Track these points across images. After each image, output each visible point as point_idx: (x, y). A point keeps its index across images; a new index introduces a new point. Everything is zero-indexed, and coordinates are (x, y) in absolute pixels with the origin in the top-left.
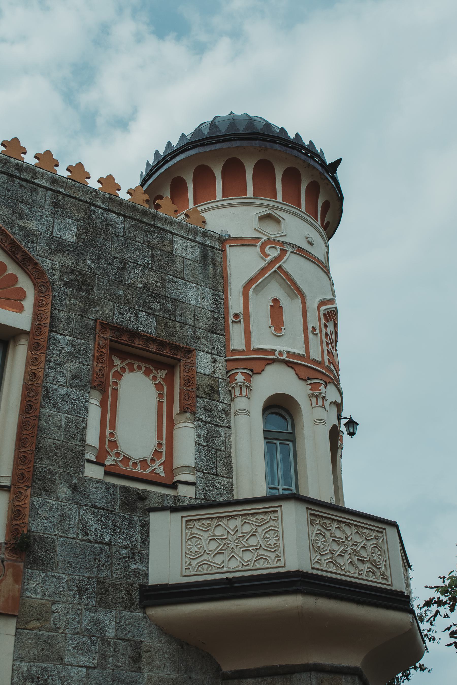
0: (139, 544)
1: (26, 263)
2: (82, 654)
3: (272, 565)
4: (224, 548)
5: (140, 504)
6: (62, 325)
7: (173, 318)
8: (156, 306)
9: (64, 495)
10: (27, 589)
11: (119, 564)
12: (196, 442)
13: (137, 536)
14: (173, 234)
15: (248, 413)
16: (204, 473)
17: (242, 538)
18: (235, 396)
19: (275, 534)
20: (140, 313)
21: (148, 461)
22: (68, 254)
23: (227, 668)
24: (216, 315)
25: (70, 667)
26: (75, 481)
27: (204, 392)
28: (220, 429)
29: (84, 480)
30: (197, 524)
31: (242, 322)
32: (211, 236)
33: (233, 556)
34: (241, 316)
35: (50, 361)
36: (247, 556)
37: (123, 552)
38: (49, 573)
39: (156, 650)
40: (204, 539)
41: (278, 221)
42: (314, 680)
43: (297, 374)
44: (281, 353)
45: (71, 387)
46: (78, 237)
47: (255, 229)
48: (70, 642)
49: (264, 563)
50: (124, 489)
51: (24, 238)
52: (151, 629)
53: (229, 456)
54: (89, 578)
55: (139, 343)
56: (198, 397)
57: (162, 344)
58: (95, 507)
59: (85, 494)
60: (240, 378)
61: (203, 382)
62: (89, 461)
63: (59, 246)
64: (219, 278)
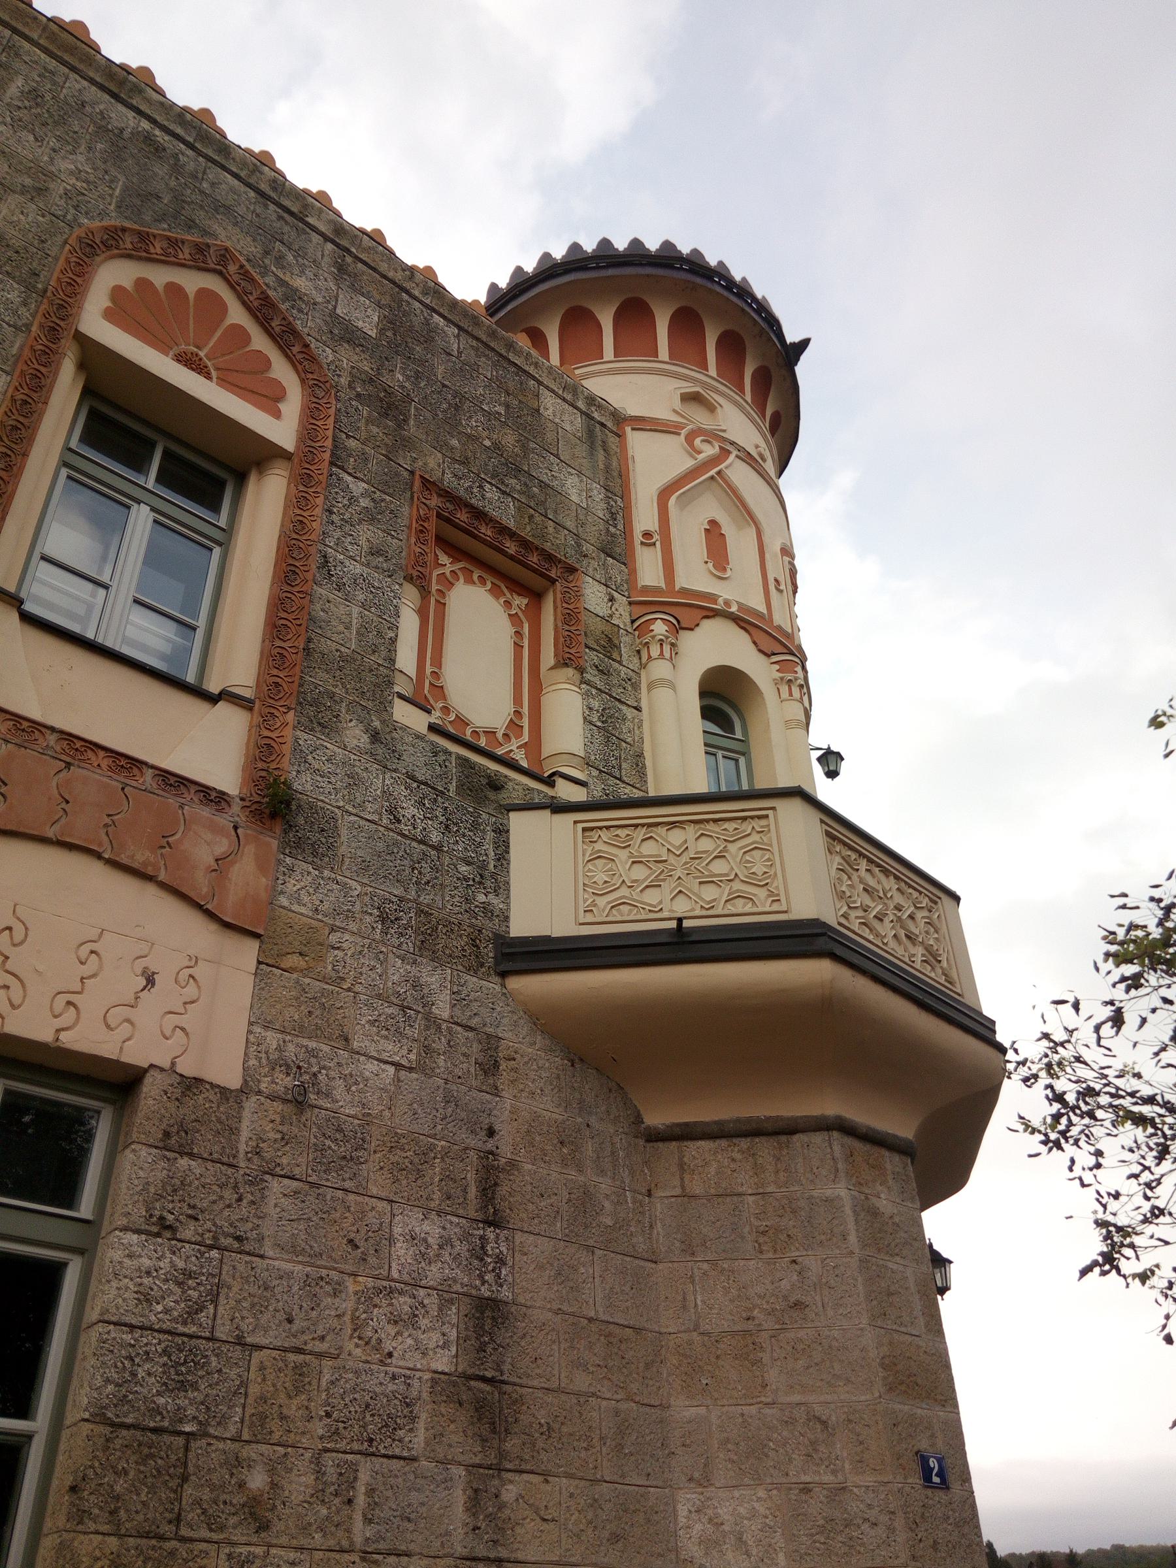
0: (492, 863)
1: (287, 339)
2: (386, 1038)
3: (760, 909)
4: (661, 877)
5: (491, 795)
6: (352, 460)
7: (543, 511)
8: (513, 481)
9: (355, 742)
10: (282, 892)
11: (456, 888)
12: (585, 718)
13: (488, 847)
14: (540, 383)
15: (673, 687)
16: (601, 771)
17: (697, 861)
18: (650, 657)
19: (762, 857)
20: (488, 486)
21: (500, 735)
22: (363, 351)
23: (656, 1119)
24: (612, 529)
25: (362, 1058)
26: (377, 724)
27: (597, 641)
28: (624, 708)
30: (605, 835)
31: (658, 544)
32: (600, 406)
33: (680, 892)
34: (656, 537)
35: (331, 512)
36: (709, 893)
37: (463, 868)
38: (326, 873)
39: (526, 1059)
40: (621, 861)
41: (711, 408)
42: (837, 1148)
43: (755, 643)
44: (727, 603)
45: (368, 565)
46: (382, 332)
47: (674, 411)
48: (365, 1010)
49: (744, 906)
50: (464, 762)
51: (286, 298)
52: (515, 1018)
53: (640, 755)
54: (401, 899)
55: (486, 531)
56: (587, 646)
57: (525, 544)
58: (413, 778)
59: (394, 751)
60: (659, 628)
62: (401, 697)
63: (348, 335)
64: (615, 474)
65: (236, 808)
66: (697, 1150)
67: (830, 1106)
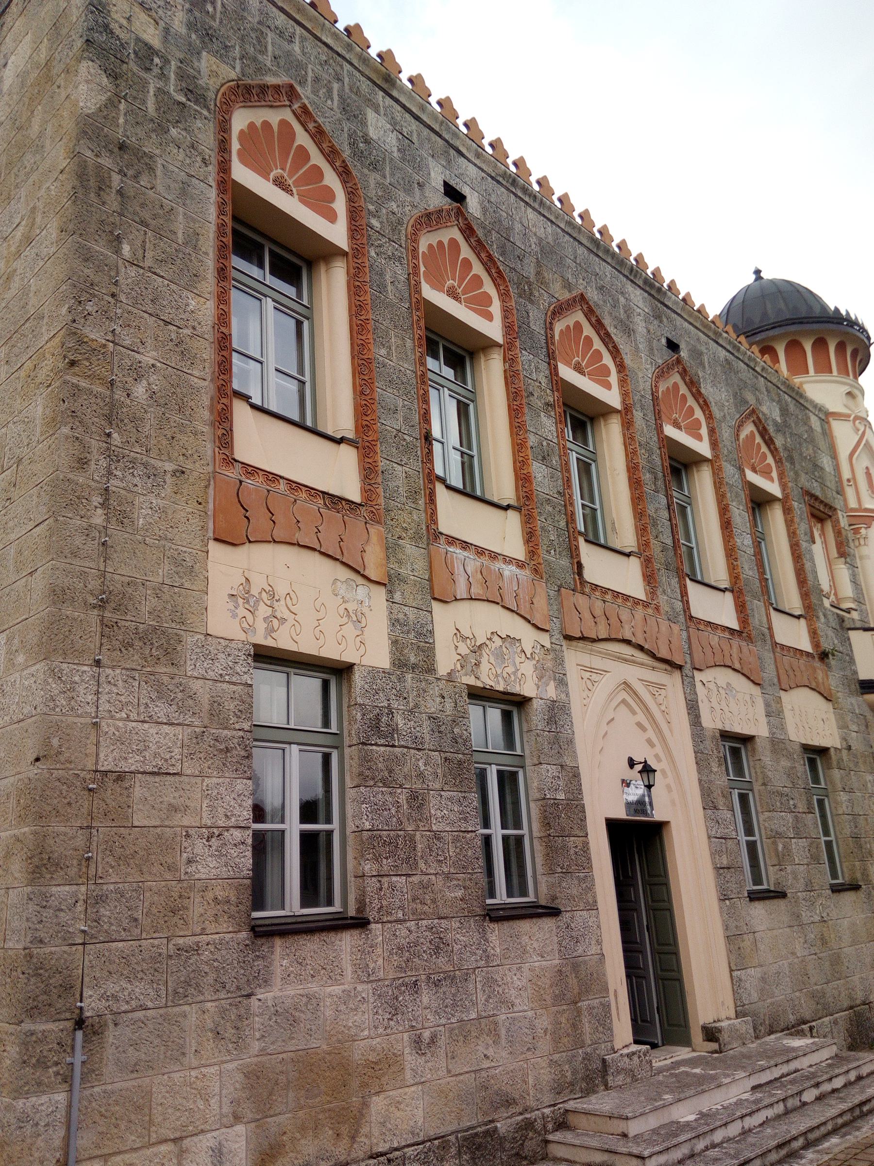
1: (769, 442)
29: (825, 609)
57: (826, 505)
65: (817, 659)
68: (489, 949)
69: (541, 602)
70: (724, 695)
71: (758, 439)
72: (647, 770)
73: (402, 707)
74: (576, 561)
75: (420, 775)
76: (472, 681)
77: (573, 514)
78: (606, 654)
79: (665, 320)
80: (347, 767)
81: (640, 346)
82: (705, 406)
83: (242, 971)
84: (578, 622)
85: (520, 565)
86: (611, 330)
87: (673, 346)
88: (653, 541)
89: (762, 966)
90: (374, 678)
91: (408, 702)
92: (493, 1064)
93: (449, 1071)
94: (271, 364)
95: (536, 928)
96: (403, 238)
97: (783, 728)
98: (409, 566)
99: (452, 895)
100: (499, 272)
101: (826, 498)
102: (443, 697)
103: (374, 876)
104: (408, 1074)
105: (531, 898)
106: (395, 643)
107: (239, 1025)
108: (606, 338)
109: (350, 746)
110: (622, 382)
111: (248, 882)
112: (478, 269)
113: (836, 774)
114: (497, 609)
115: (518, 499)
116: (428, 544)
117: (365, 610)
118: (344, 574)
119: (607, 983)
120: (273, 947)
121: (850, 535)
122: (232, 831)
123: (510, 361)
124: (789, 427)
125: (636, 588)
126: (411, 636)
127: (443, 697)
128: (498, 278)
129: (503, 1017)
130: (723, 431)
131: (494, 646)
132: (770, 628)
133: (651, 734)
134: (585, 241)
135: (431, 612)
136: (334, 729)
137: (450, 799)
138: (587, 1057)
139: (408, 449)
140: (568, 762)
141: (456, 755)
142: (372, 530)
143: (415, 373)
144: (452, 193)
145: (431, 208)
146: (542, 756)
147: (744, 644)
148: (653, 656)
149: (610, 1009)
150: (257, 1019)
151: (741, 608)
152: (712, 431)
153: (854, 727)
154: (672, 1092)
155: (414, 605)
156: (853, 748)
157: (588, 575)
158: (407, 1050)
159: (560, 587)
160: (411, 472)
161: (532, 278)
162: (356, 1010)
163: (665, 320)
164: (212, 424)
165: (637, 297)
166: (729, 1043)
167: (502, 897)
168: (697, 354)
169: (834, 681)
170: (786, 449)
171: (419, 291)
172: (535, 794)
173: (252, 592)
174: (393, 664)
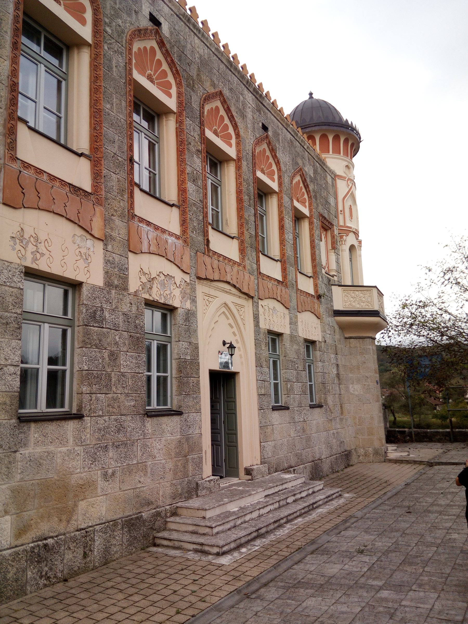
1: (306, 187)
23: (347, 336)
29: (323, 274)
36: (362, 304)
57: (329, 222)
61: (336, 237)
66: (352, 340)
67: (370, 335)
68: (145, 430)
69: (186, 258)
70: (271, 313)
71: (301, 185)
72: (231, 347)
73: (109, 308)
74: (206, 238)
75: (116, 343)
76: (147, 296)
77: (207, 213)
78: (217, 288)
79: (262, 113)
80: (76, 337)
81: (249, 126)
82: (278, 163)
83: (12, 439)
84: (205, 271)
85: (177, 237)
86: (234, 114)
87: (265, 128)
88: (245, 232)
89: (275, 441)
90: (94, 290)
91: (112, 305)
92: (143, 485)
93: (120, 489)
94: (42, 104)
95: (170, 421)
96: (124, 41)
97: (296, 330)
98: (117, 232)
99: (129, 404)
100: (177, 71)
101: (330, 219)
102: (131, 304)
103: (88, 393)
104: (99, 490)
105: (169, 407)
106: (106, 273)
107: (9, 466)
108: (231, 118)
109: (78, 326)
110: (238, 144)
111: (17, 394)
112: (165, 66)
113: (318, 353)
114: (164, 259)
115: (179, 201)
116: (128, 221)
117: (91, 253)
118: (79, 232)
119: (202, 448)
120: (30, 427)
121: (338, 239)
122: (9, 367)
123: (180, 123)
124: (317, 180)
125: (235, 255)
126: (116, 270)
127: (131, 304)
128: (176, 74)
129: (150, 463)
130: (285, 178)
131: (160, 279)
132: (296, 282)
133: (235, 329)
134: (224, 61)
135: (128, 258)
136: (70, 316)
137: (131, 356)
138: (189, 482)
139: (119, 165)
140: (194, 341)
141: (136, 334)
142: (97, 209)
143: (126, 121)
144: (154, 20)
145: (141, 27)
146: (181, 337)
147: (283, 288)
148: (240, 291)
149: (202, 459)
150: (19, 463)
151: (284, 270)
152: (280, 177)
153: (329, 332)
154: (228, 498)
155: (118, 253)
156: (327, 342)
157: (212, 247)
158: (99, 479)
159: (197, 251)
160: (121, 179)
161: (195, 77)
162: (74, 459)
163: (262, 113)
164: (5, 135)
165: (249, 97)
166: (256, 476)
167: (154, 405)
168: (276, 134)
169: (322, 309)
170: (314, 191)
171: (131, 74)
172: (175, 356)
173: (25, 237)
174: (105, 284)
